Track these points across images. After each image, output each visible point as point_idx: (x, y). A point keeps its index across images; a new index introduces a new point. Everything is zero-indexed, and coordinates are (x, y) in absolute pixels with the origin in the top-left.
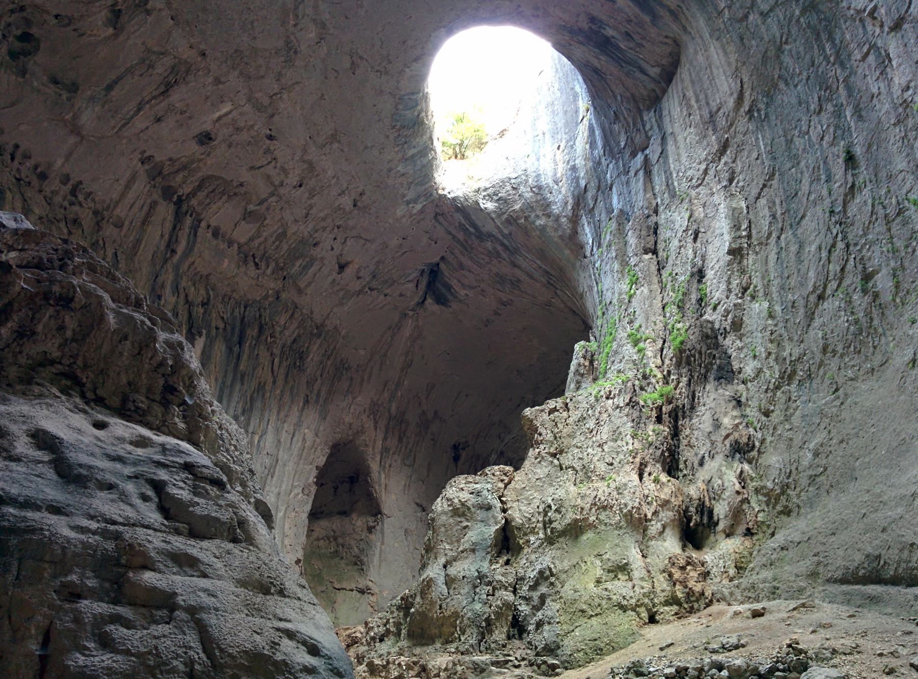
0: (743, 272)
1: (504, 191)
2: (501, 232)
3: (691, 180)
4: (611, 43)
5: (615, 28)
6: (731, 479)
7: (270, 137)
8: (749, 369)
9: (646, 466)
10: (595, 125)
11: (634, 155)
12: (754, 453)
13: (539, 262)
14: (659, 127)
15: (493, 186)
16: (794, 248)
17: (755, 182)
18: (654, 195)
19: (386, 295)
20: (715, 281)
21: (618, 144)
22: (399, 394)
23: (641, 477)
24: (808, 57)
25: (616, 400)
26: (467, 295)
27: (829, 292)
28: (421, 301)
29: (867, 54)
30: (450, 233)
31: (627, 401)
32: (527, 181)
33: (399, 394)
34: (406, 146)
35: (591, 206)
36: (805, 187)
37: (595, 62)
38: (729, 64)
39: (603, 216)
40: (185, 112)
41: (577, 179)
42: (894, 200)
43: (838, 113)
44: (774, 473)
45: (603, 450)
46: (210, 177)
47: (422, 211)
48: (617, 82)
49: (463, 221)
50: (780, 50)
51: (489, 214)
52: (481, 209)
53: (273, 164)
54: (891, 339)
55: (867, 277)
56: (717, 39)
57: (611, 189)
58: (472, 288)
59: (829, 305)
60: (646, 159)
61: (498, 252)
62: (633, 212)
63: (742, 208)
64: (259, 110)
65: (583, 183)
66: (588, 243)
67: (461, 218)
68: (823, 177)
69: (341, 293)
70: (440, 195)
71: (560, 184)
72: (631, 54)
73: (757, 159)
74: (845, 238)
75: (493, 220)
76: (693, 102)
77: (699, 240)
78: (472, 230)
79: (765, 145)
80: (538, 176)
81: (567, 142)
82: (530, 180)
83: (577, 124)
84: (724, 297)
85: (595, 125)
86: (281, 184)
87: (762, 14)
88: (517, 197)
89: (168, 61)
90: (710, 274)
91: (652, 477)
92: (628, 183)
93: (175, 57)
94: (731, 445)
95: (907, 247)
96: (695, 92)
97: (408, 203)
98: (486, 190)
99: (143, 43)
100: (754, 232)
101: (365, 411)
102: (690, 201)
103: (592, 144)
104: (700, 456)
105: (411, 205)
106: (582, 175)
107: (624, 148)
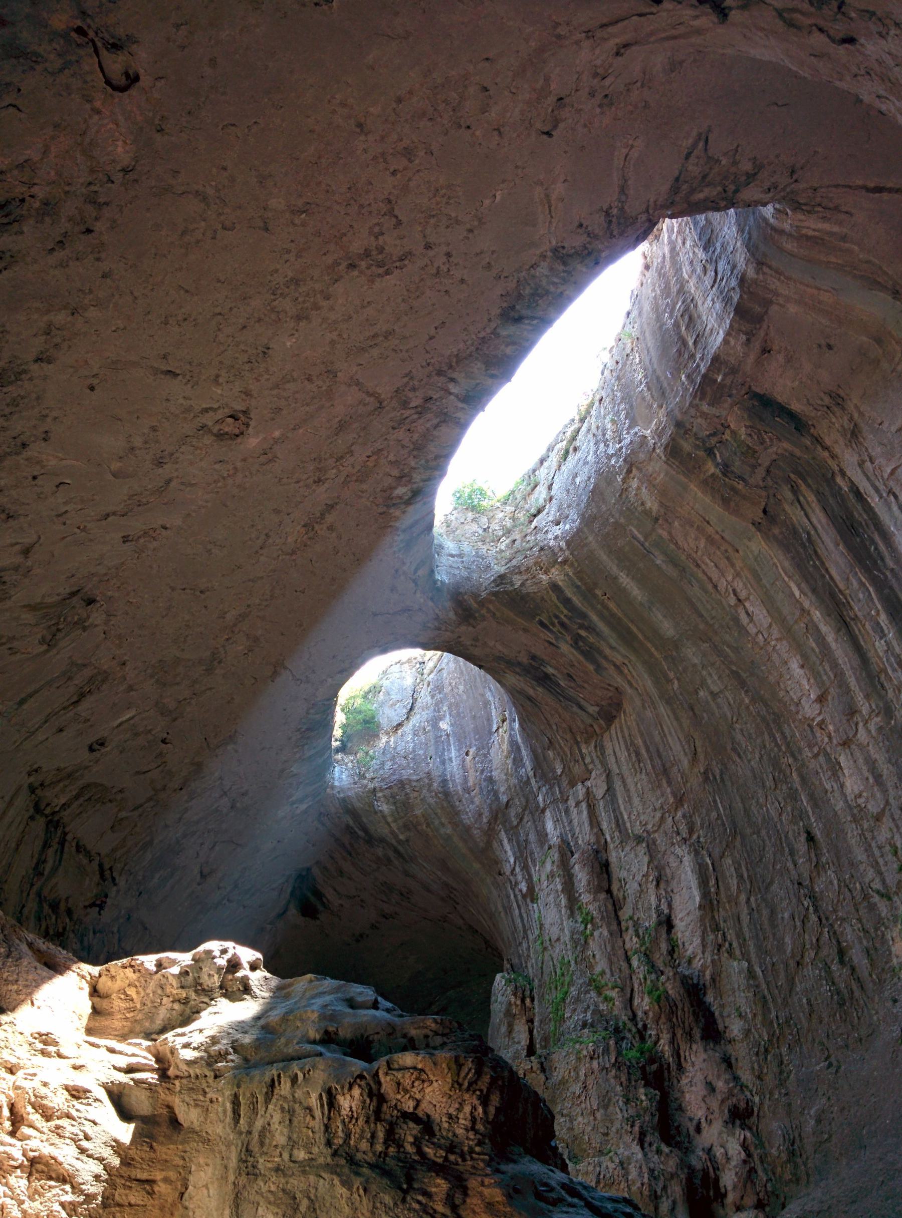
0: (716, 928)
2: (396, 836)
3: (645, 825)
4: (550, 679)
5: (556, 668)
6: (734, 1148)
7: (164, 741)
8: (735, 1028)
9: (645, 1136)
10: (520, 740)
11: (572, 784)
12: (754, 1119)
13: (439, 873)
14: (602, 763)
15: (390, 788)
16: (765, 912)
17: (718, 841)
18: (601, 830)
19: (244, 907)
20: (687, 934)
21: (553, 770)
23: (643, 1148)
24: (759, 741)
25: (601, 1060)
26: (342, 906)
27: (807, 959)
29: (816, 756)
31: (613, 1060)
32: (430, 785)
34: (306, 747)
35: (515, 823)
36: (769, 855)
37: (531, 692)
38: (681, 725)
39: (532, 837)
40: (89, 720)
41: (496, 793)
42: (858, 885)
43: (793, 796)
44: (778, 1141)
45: (595, 1119)
46: (88, 785)
47: (305, 812)
48: (553, 712)
49: (351, 823)
50: (731, 727)
53: (161, 768)
54: (874, 1012)
55: (841, 953)
56: (667, 703)
57: (543, 811)
58: (349, 897)
59: (811, 972)
60: (588, 793)
61: (389, 860)
62: (577, 843)
63: (707, 863)
64: (162, 714)
65: (504, 799)
66: (508, 861)
68: (787, 850)
71: (473, 794)
72: (572, 692)
73: (717, 819)
74: (816, 910)
75: (388, 824)
76: (643, 751)
77: (662, 885)
78: (360, 833)
79: (723, 807)
80: (444, 782)
81: (478, 749)
82: (435, 785)
83: (491, 733)
84: (700, 952)
85: (520, 740)
86: (164, 788)
87: (712, 693)
89: (87, 672)
90: (680, 924)
91: (654, 1148)
92: (567, 811)
93: (95, 668)
94: (729, 1111)
95: (876, 929)
96: (645, 742)
97: (293, 803)
98: (381, 790)
99: (70, 657)
100: (722, 888)
102: (648, 846)
103: (518, 762)
104: (695, 1122)
105: (295, 806)
106: (502, 789)
107: (561, 775)
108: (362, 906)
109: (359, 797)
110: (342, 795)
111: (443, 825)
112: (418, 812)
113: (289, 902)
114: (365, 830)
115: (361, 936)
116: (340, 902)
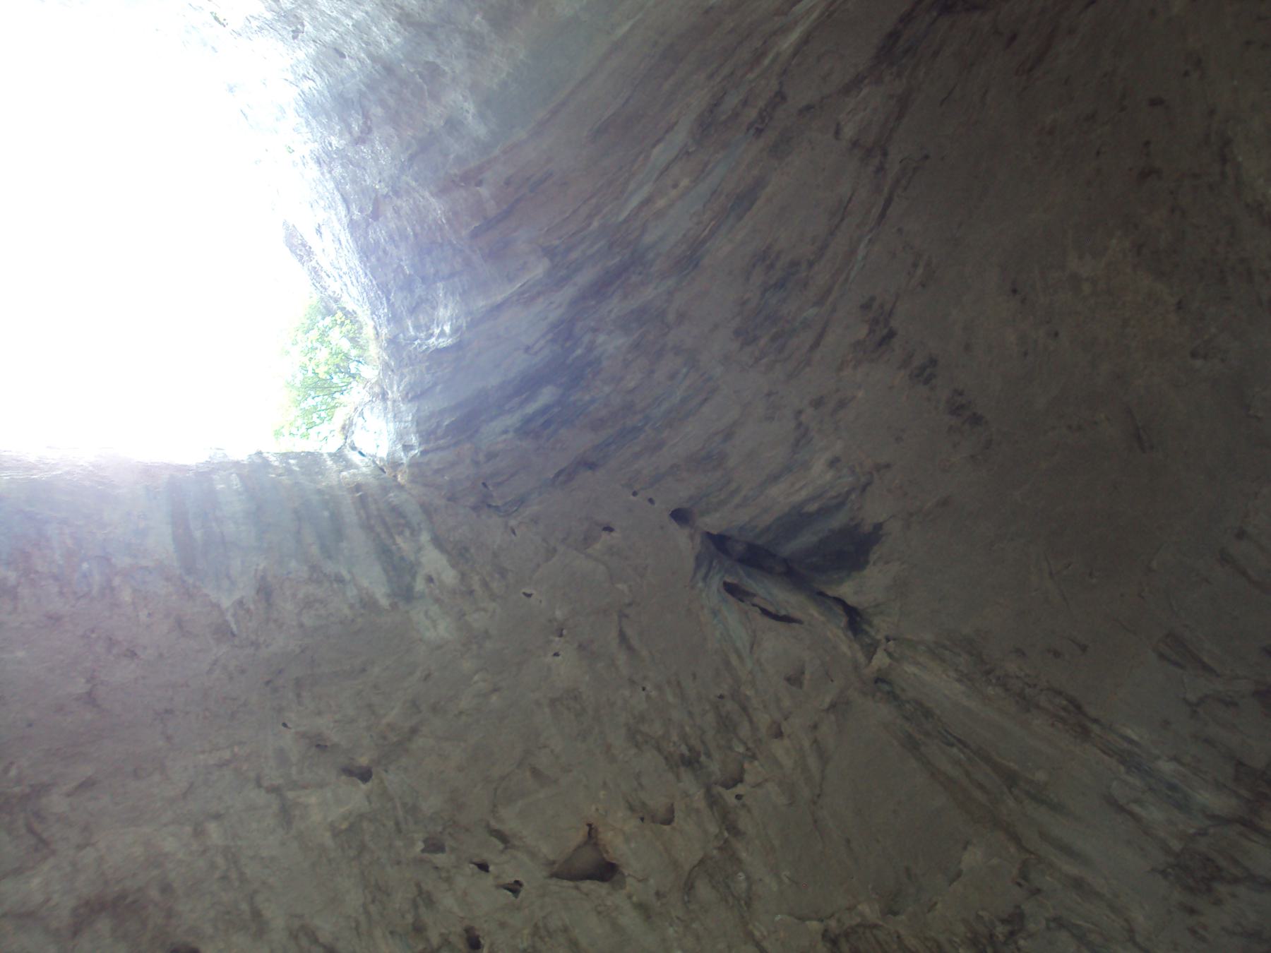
1: (391, 249)
13: (660, 155)
15: (384, 288)
19: (779, 734)
22: (1166, 767)
26: (833, 463)
28: (844, 621)
30: (566, 476)
33: (1166, 767)
47: (459, 554)
49: (512, 420)
51: (473, 324)
52: (458, 346)
67: (498, 425)
69: (704, 890)
70: (413, 480)
75: (499, 307)
88: (404, 204)
97: (405, 594)
98: (395, 319)
101: (1192, 911)
105: (420, 585)
108: (842, 404)
109: (416, 394)
110: (414, 440)
111: (453, 125)
112: (437, 208)
113: (820, 597)
114: (528, 385)
115: (956, 410)
116: (819, 465)
